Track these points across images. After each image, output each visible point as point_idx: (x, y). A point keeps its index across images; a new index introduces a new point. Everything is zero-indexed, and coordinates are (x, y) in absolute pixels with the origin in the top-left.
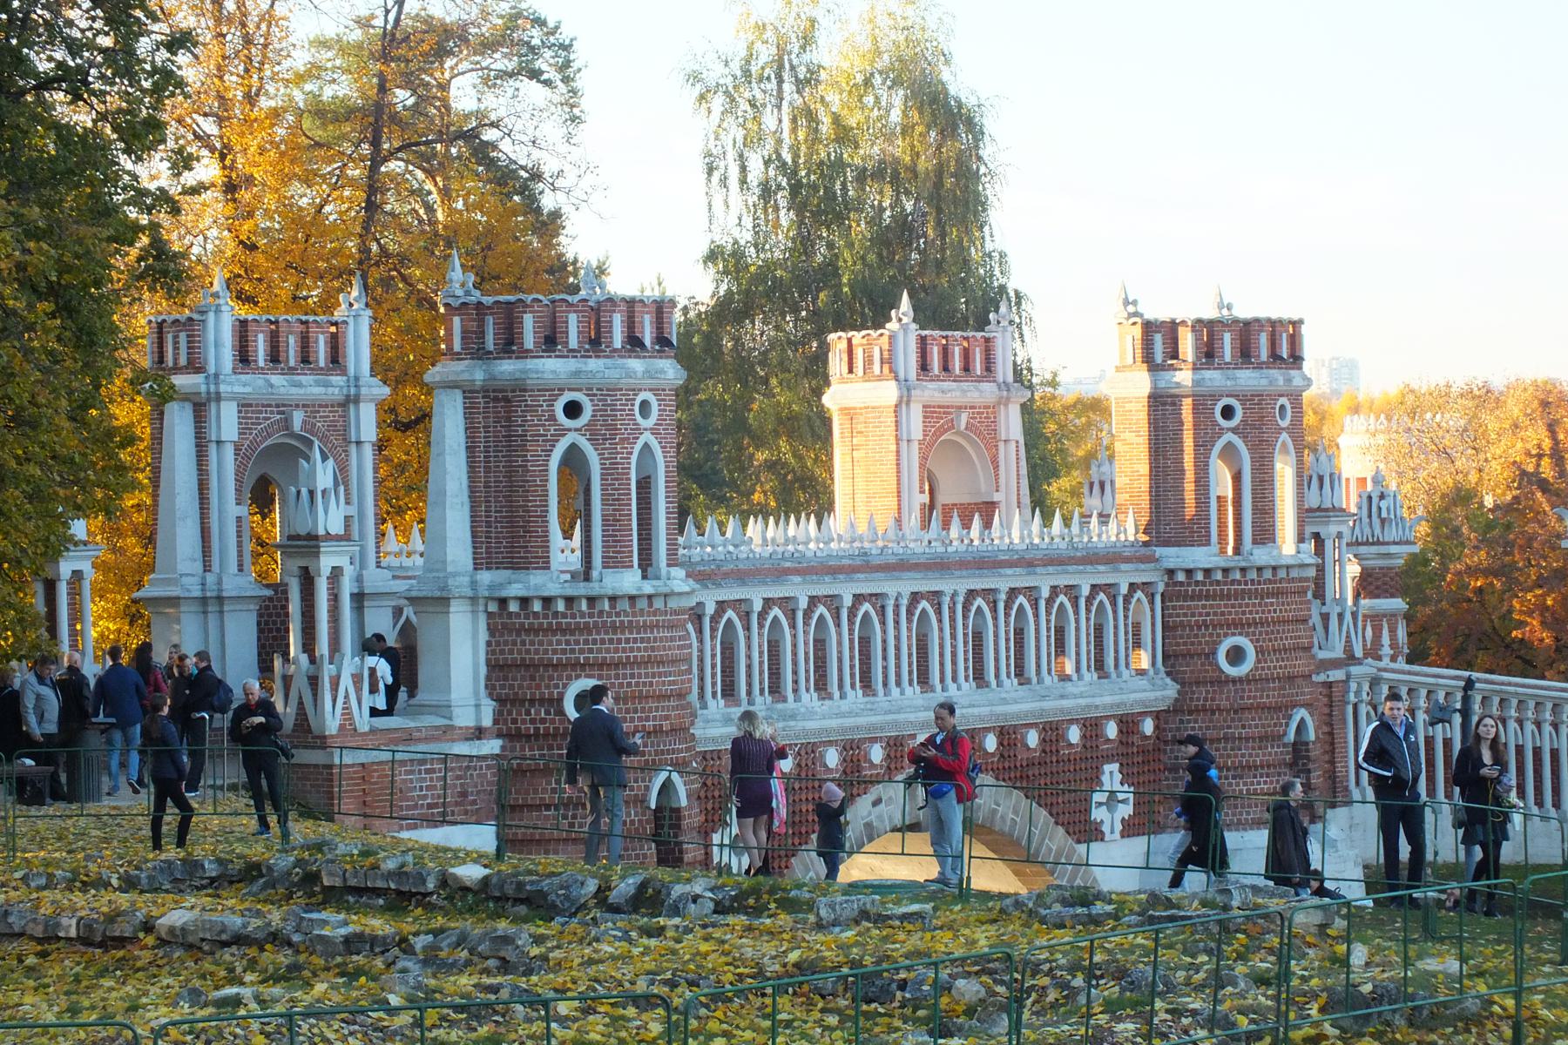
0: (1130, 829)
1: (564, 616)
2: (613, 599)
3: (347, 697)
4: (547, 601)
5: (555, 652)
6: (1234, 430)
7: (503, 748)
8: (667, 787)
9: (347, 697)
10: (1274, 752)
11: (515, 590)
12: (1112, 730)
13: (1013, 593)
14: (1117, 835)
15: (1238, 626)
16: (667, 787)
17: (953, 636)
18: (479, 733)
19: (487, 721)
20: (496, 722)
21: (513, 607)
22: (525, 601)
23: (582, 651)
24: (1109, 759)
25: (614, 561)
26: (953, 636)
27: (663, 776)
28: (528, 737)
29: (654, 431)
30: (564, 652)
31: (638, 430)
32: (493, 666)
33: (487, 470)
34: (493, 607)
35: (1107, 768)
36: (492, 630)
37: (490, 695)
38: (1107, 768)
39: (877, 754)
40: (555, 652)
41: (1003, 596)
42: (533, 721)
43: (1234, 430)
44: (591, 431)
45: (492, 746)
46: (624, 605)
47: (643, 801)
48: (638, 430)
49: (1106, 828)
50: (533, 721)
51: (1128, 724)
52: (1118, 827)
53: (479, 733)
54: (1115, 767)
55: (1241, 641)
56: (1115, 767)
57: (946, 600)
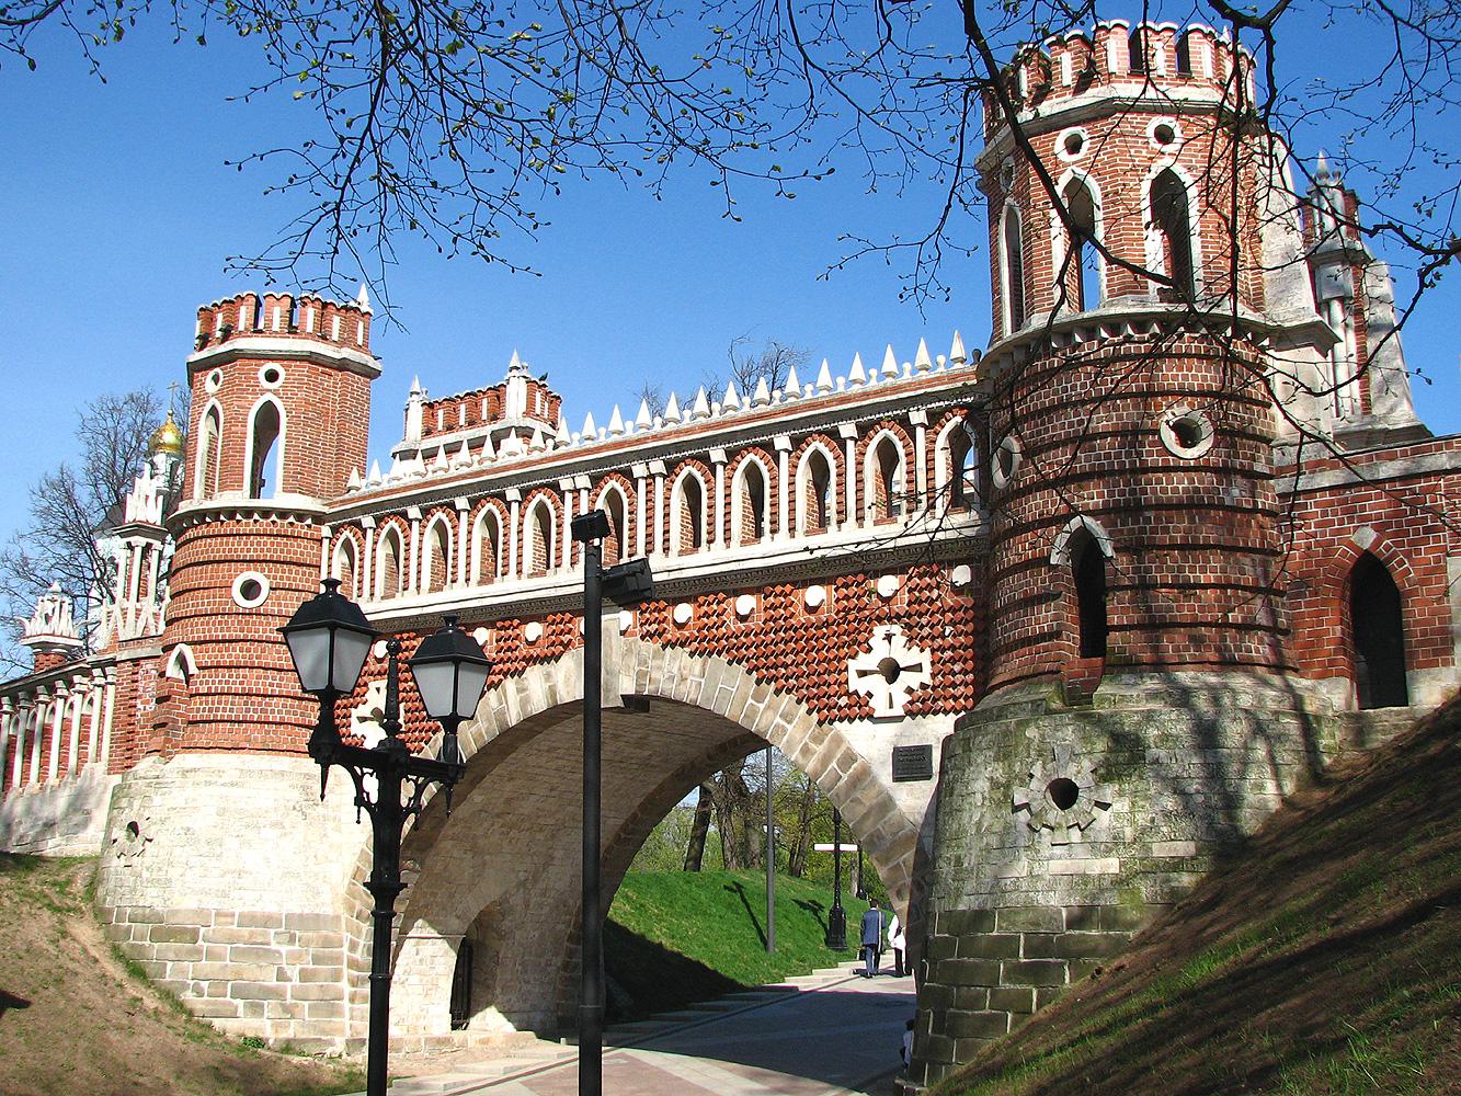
14: (898, 711)
35: (880, 631)
52: (902, 699)
56: (896, 629)
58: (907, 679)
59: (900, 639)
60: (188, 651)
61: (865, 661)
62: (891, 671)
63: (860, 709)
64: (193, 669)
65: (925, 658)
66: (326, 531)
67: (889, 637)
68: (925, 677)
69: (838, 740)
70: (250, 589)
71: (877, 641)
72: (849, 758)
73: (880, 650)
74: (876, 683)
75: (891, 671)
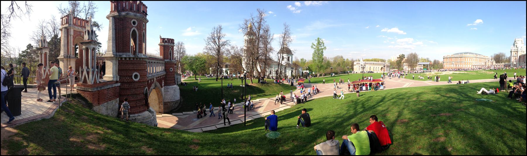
1: (133, 61)
2: (140, 58)
3: (95, 76)
4: (130, 58)
5: (131, 67)
7: (121, 84)
9: (95, 76)
11: (124, 56)
15: (171, 67)
18: (117, 82)
19: (118, 80)
20: (119, 80)
21: (124, 59)
22: (125, 58)
23: (135, 67)
28: (125, 83)
30: (132, 67)
32: (119, 70)
33: (119, 34)
34: (119, 59)
37: (119, 75)
40: (131, 67)
42: (127, 80)
45: (119, 84)
50: (127, 80)
53: (117, 82)
55: (172, 68)
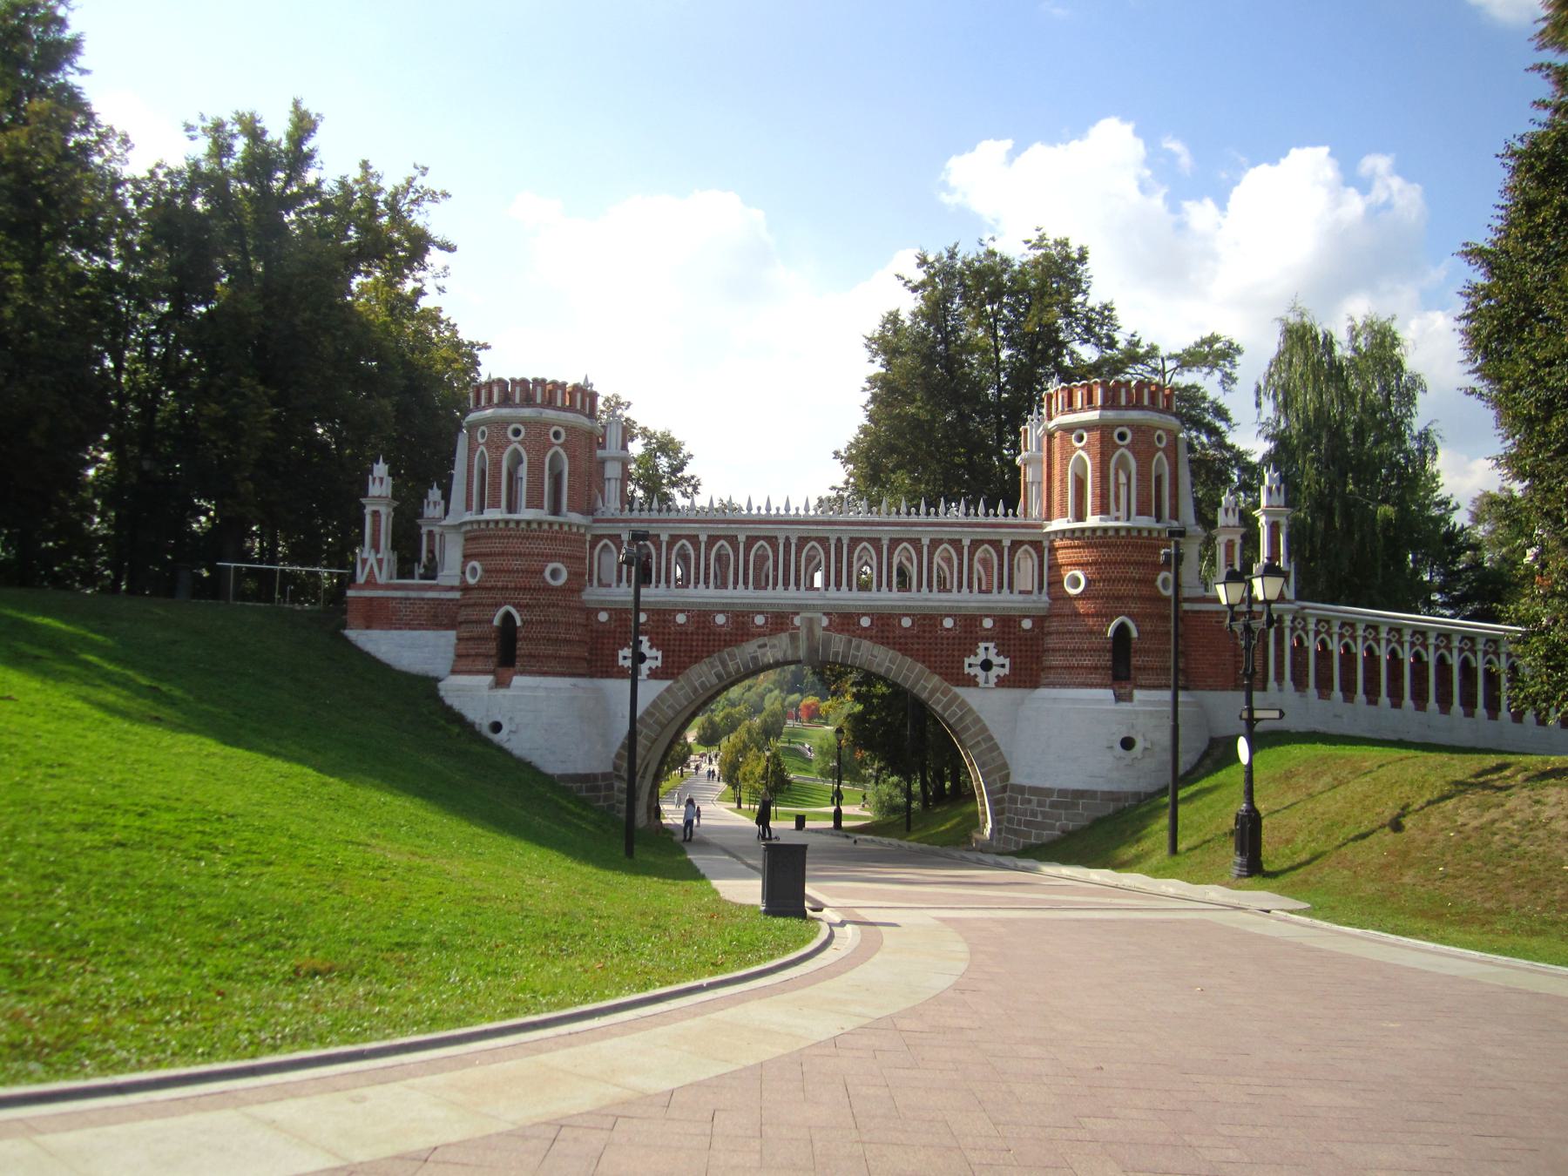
0: (1002, 682)
3: (372, 567)
6: (1082, 448)
8: (508, 617)
9: (372, 567)
10: (1096, 641)
12: (988, 623)
13: (895, 543)
16: (508, 617)
17: (839, 561)
24: (986, 639)
25: (495, 504)
26: (839, 561)
27: (502, 611)
29: (519, 442)
31: (509, 442)
35: (982, 645)
36: (466, 540)
38: (982, 645)
39: (760, 620)
41: (885, 543)
43: (1082, 448)
44: (486, 444)
45: (457, 595)
46: (492, 525)
47: (491, 621)
48: (509, 442)
49: (981, 680)
51: (1006, 622)
52: (993, 681)
53: (452, 588)
54: (991, 645)
56: (991, 645)
57: (833, 543)
58: (995, 671)
59: (993, 651)
60: (513, 611)
61: (972, 660)
62: (987, 665)
63: (971, 682)
64: (519, 623)
65: (1007, 662)
66: (588, 537)
67: (987, 649)
68: (1006, 671)
69: (956, 697)
70: (555, 574)
71: (981, 651)
72: (963, 704)
73: (982, 655)
74: (977, 671)
75: (987, 665)
